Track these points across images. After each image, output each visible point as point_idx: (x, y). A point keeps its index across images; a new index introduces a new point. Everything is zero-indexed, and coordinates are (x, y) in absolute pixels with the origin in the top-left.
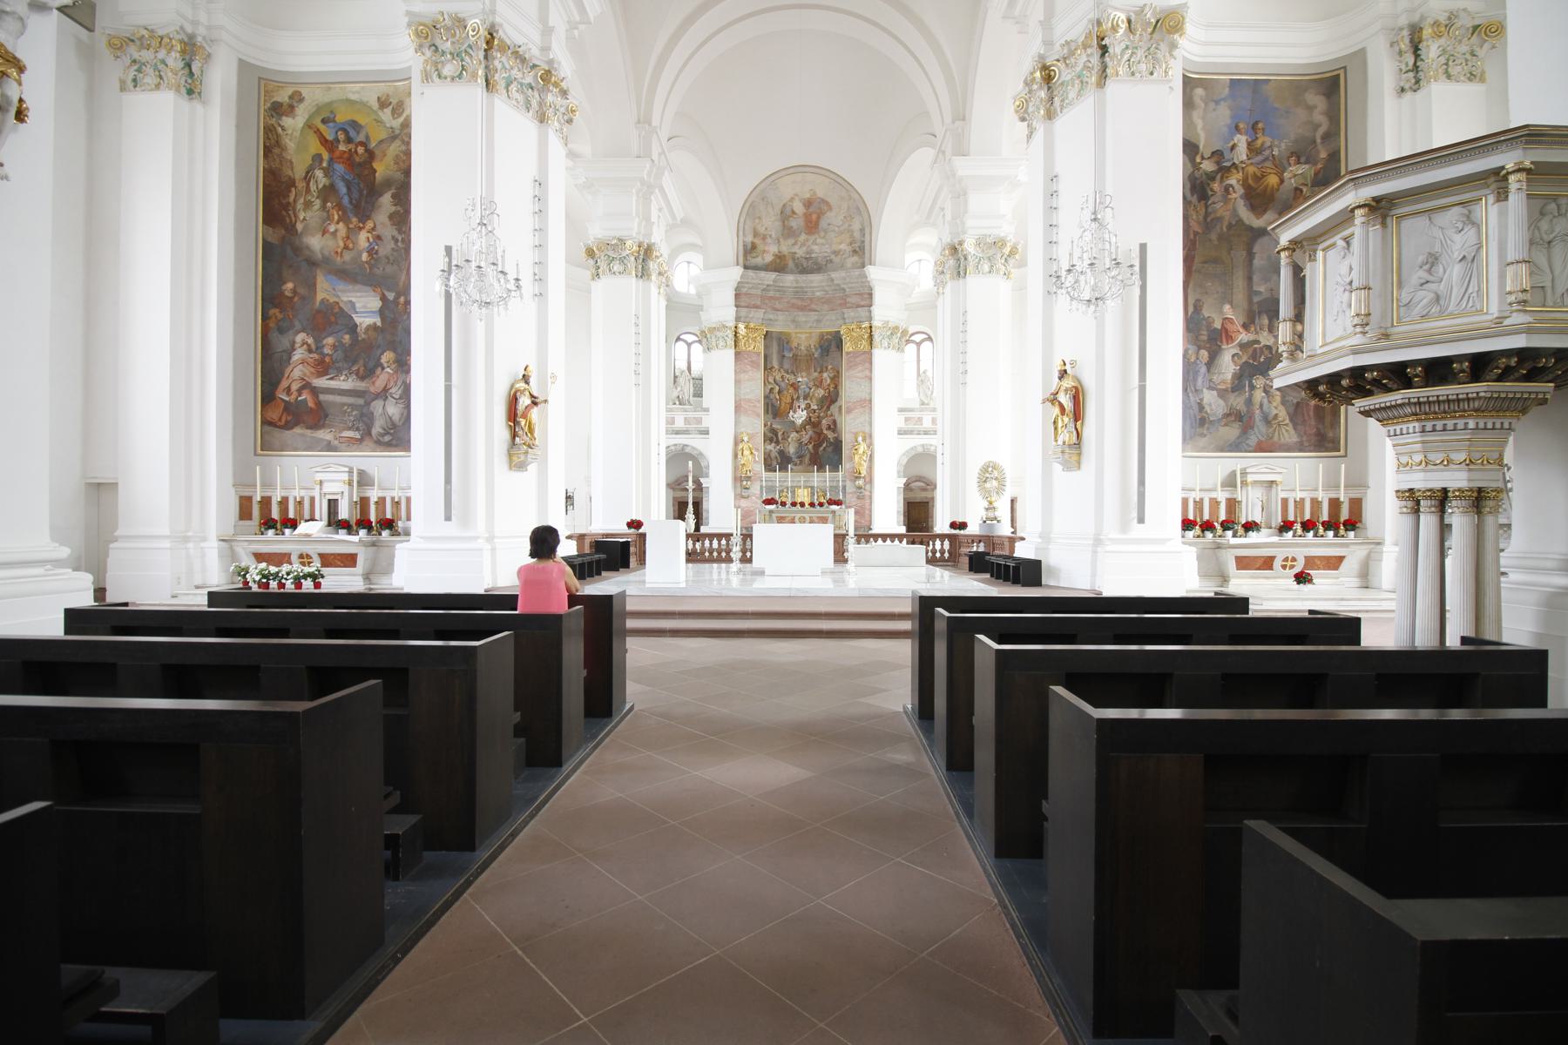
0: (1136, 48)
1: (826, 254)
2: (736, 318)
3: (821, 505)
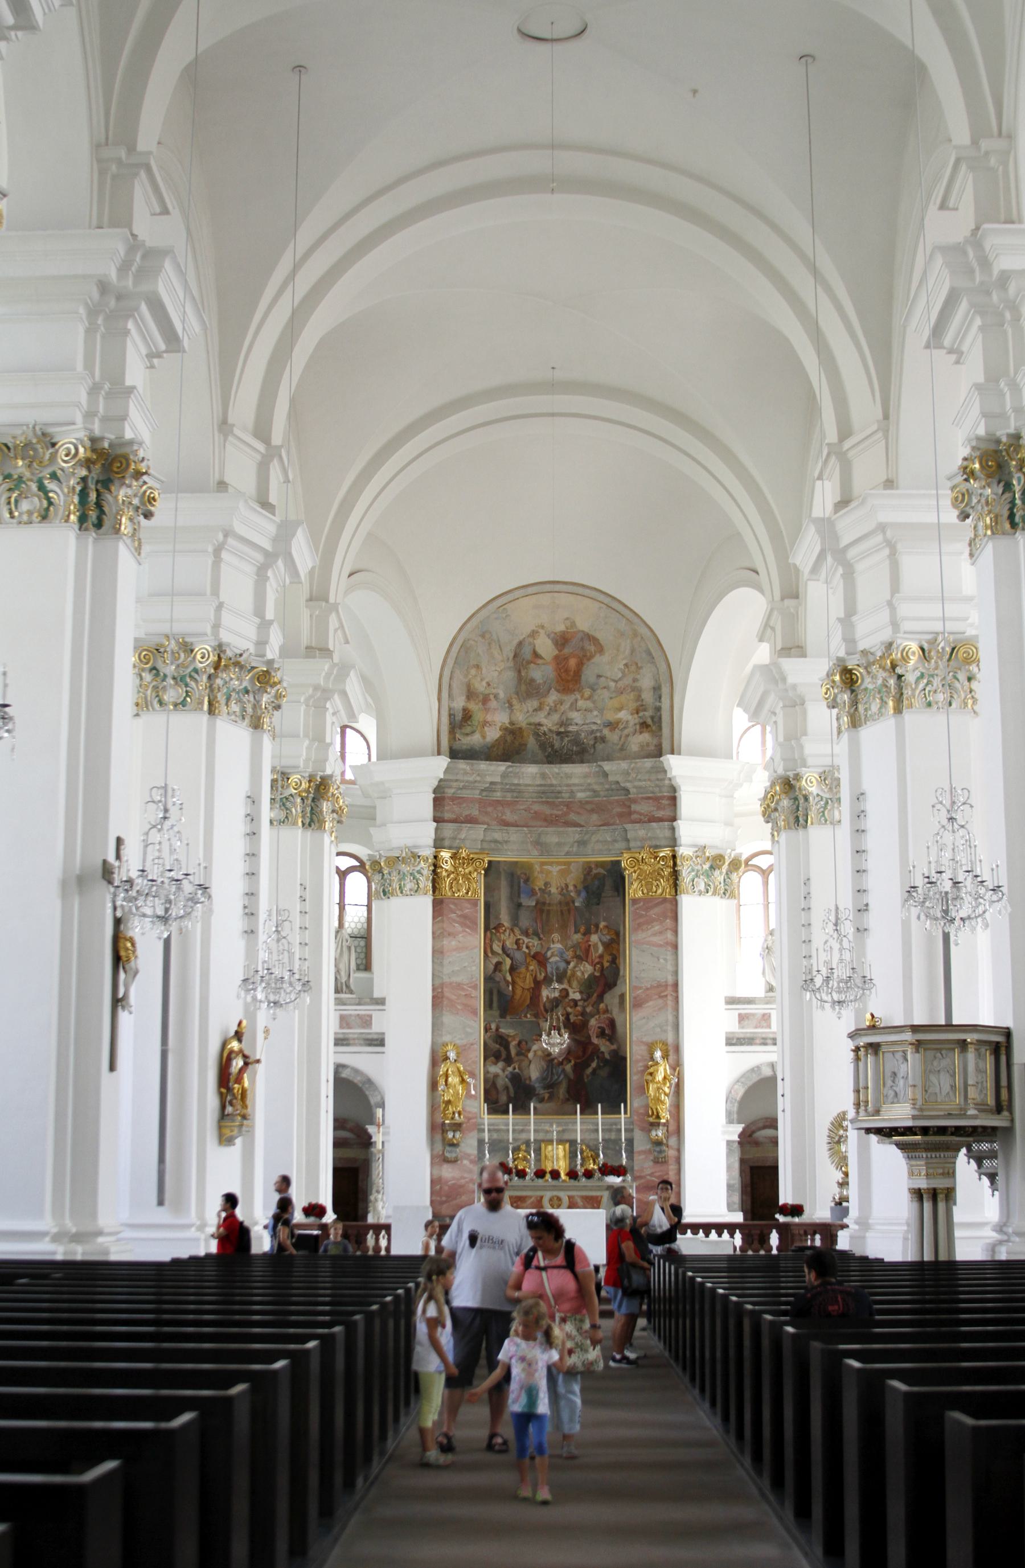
0: (932, 676)
1: (594, 727)
2: (435, 840)
3: (588, 1174)
